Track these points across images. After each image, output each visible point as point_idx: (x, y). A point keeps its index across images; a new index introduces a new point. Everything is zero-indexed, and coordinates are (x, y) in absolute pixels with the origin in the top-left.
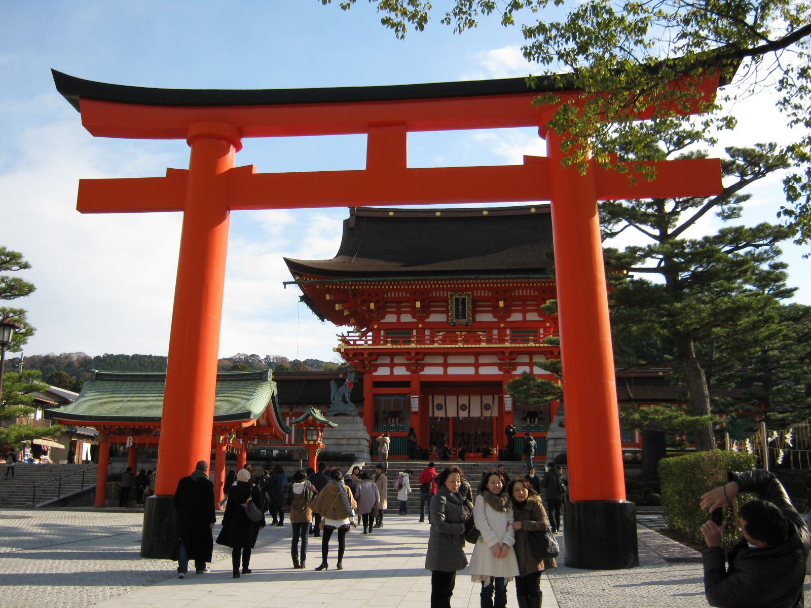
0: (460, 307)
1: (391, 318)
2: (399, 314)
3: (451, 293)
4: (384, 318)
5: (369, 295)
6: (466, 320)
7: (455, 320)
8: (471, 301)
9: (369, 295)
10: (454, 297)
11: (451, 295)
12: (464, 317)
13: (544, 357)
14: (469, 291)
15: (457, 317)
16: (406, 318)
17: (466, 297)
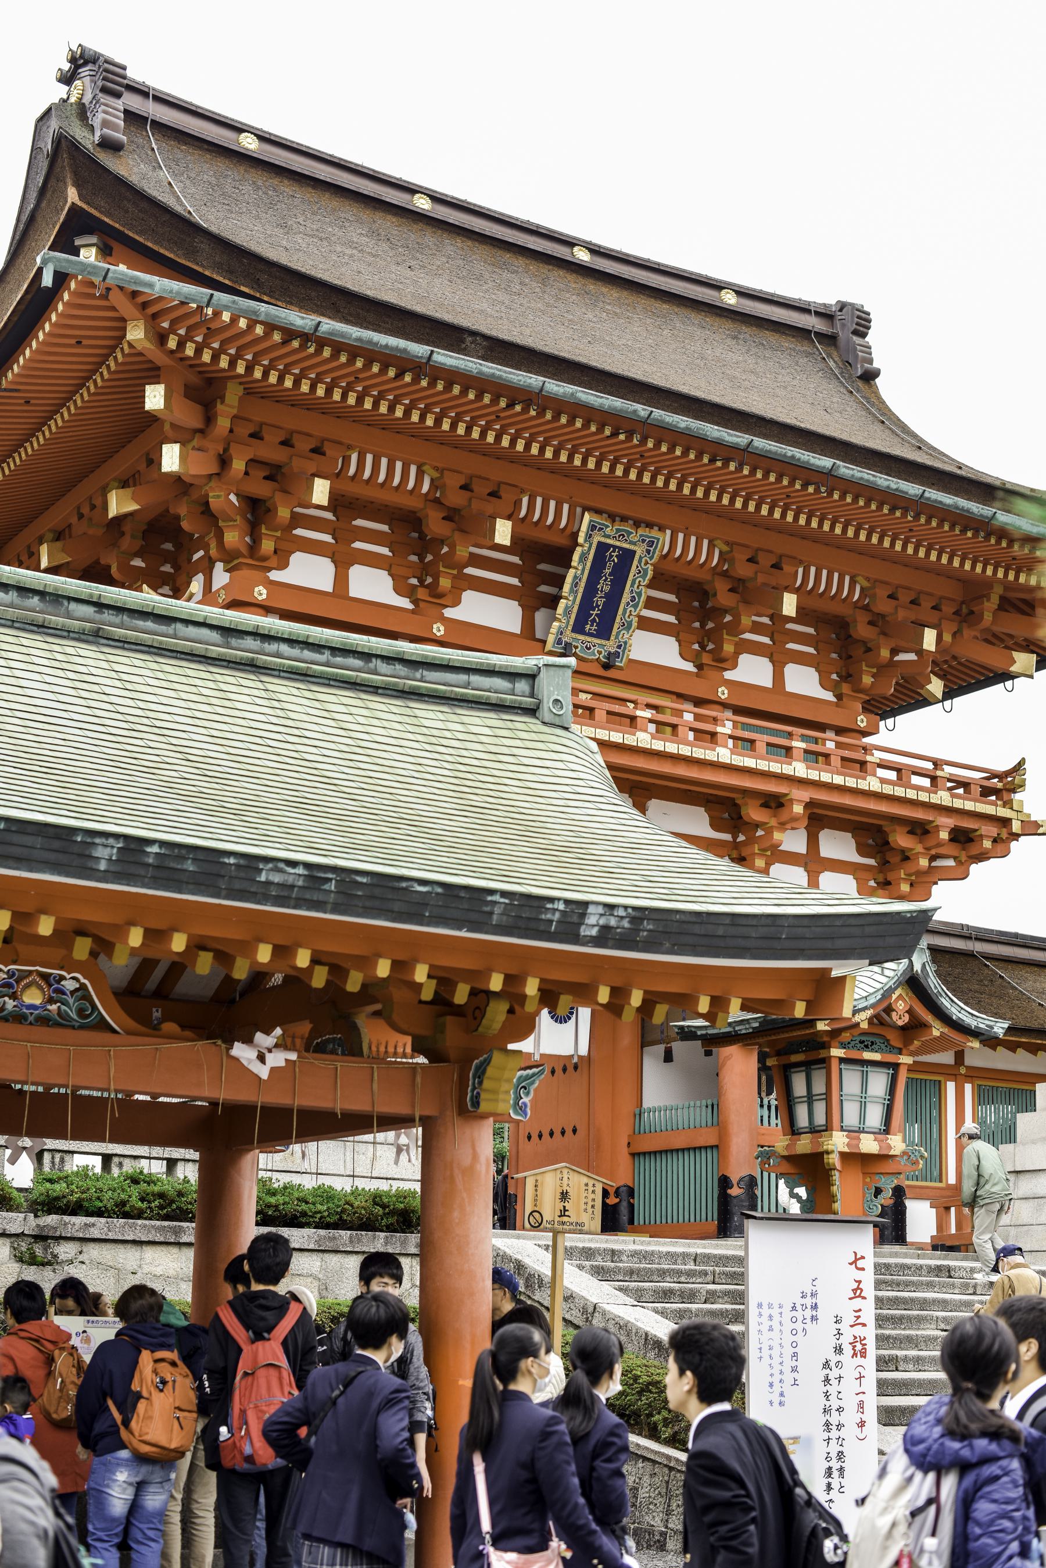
0: (604, 586)
1: (309, 572)
2: (343, 561)
3: (597, 519)
4: (283, 565)
5: (286, 443)
6: (611, 646)
7: (569, 636)
8: (650, 574)
9: (286, 443)
10: (597, 538)
11: (592, 527)
12: (604, 632)
13: (852, 844)
14: (650, 525)
15: (579, 628)
16: (371, 585)
17: (640, 550)
